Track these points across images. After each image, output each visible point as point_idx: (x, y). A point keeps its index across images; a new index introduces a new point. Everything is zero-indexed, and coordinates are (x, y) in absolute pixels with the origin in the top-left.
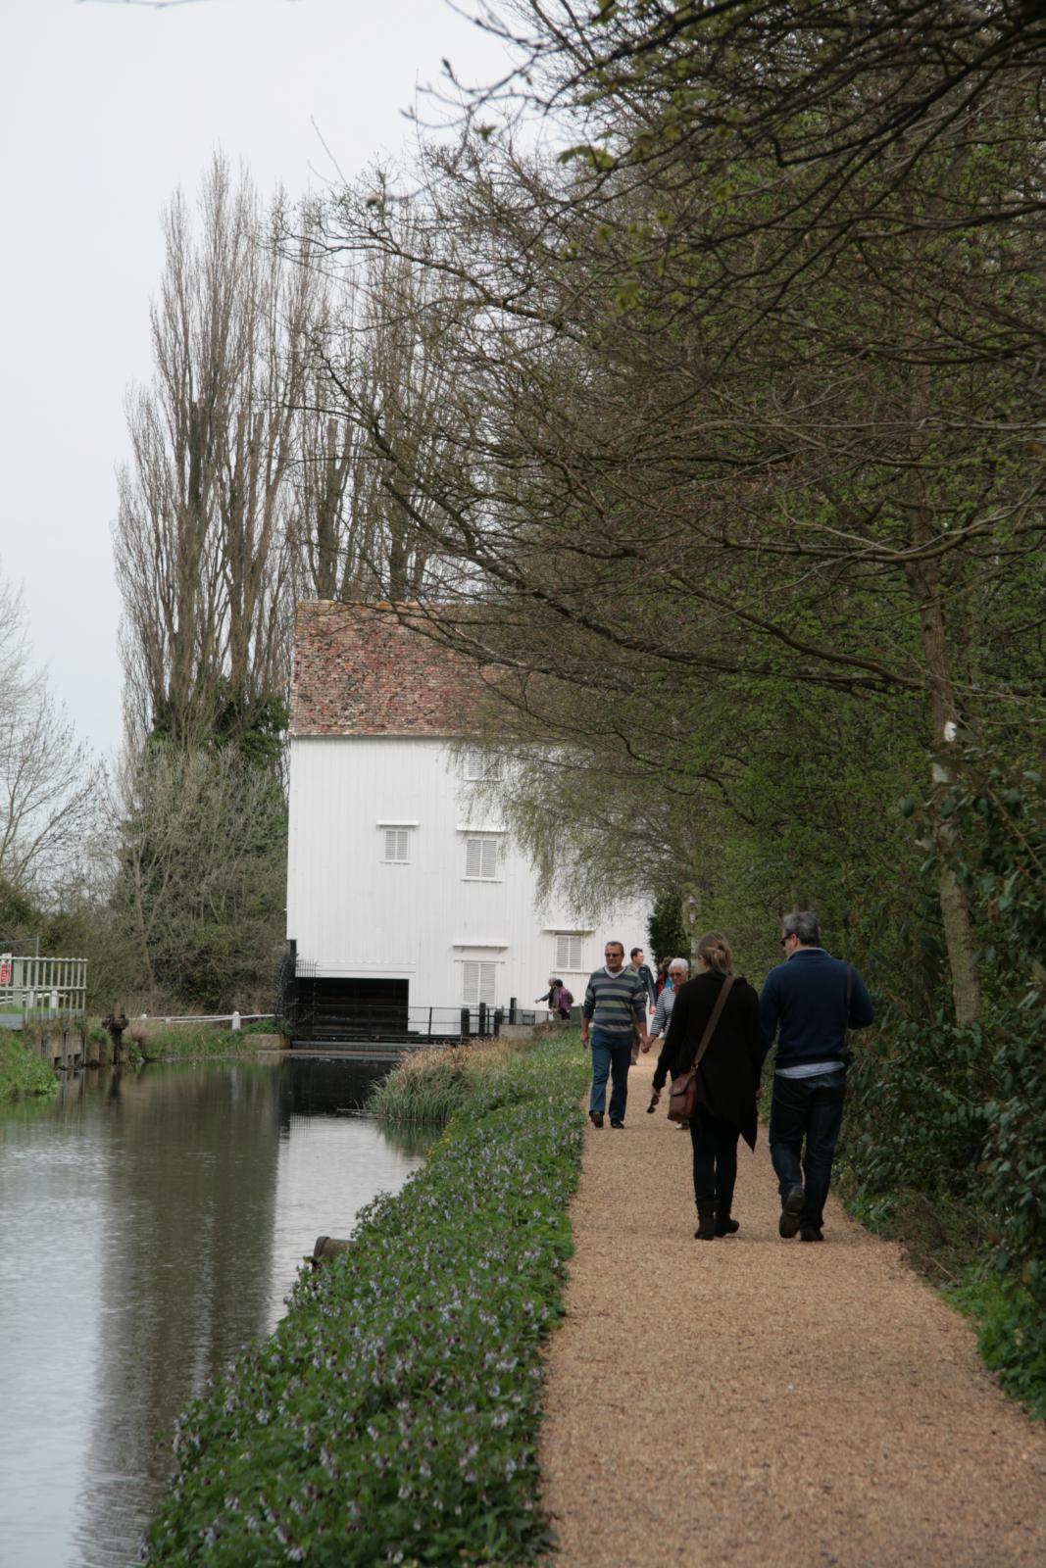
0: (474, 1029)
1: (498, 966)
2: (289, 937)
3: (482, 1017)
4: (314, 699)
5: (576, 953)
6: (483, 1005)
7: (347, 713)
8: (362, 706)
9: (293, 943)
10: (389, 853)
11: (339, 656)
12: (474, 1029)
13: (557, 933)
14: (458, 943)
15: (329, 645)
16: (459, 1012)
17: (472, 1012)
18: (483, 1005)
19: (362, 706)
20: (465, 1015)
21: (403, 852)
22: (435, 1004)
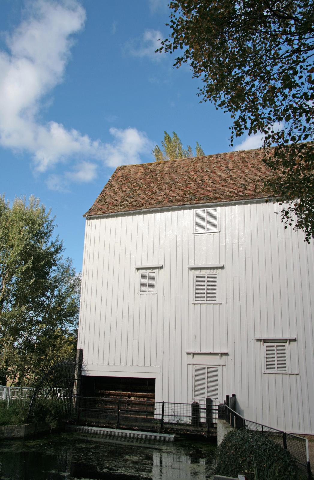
0: (203, 420)
1: (220, 369)
2: (79, 347)
3: (209, 410)
4: (107, 200)
5: (282, 356)
6: (209, 401)
7: (123, 203)
8: (134, 200)
9: (81, 351)
10: (143, 288)
11: (129, 182)
12: (203, 420)
13: (265, 341)
14: (191, 350)
15: (126, 179)
16: (191, 405)
17: (201, 407)
18: (209, 401)
19: (134, 200)
20: (196, 408)
21: (151, 286)
22: (174, 399)
